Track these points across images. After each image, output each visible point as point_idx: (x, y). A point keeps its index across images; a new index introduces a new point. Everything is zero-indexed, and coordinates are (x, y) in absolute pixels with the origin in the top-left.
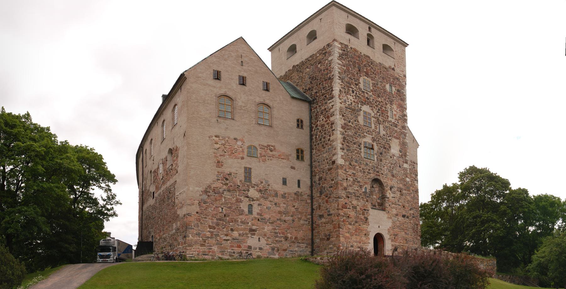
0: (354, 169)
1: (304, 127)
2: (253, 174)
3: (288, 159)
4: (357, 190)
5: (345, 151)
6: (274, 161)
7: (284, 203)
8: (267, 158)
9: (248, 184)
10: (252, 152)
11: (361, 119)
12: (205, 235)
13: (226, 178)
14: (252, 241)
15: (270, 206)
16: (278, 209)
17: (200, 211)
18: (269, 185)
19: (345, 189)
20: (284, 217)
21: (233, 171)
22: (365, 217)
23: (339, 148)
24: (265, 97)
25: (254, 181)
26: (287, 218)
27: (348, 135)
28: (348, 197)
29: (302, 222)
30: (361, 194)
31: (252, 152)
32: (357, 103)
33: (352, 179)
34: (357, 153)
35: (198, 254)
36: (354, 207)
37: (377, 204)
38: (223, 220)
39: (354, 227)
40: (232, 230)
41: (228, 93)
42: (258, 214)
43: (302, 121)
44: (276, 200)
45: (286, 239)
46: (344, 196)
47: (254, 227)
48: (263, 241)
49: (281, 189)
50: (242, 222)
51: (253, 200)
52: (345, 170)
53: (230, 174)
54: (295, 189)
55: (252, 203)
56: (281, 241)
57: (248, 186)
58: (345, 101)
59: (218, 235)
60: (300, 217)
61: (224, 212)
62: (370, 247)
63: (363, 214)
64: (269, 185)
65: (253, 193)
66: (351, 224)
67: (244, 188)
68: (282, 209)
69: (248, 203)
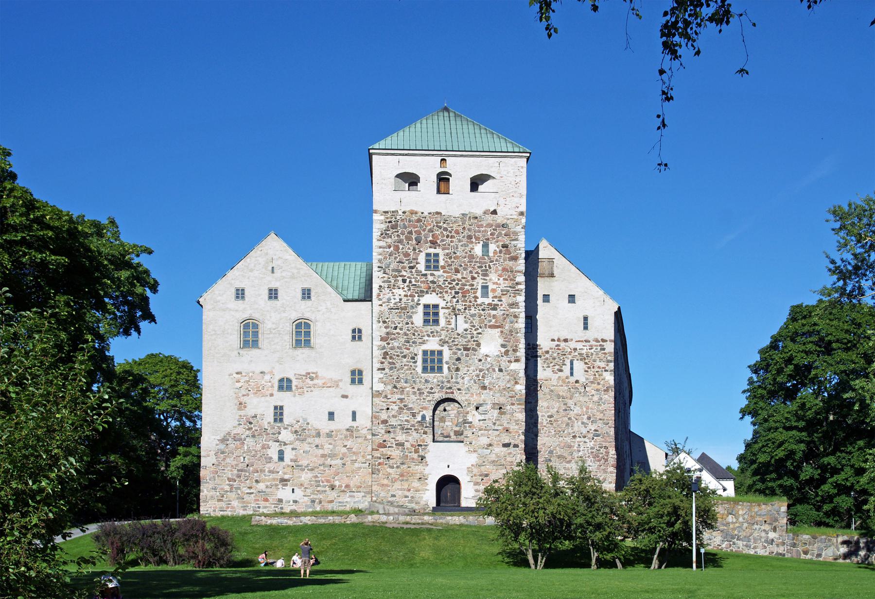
0: (402, 392)
1: (363, 338)
3: (337, 386)
4: (407, 421)
5: (387, 370)
6: (316, 392)
8: (305, 389)
9: (279, 425)
10: (285, 385)
14: (285, 493)
15: (309, 449)
16: (321, 452)
17: (216, 463)
18: (308, 424)
19: (385, 422)
20: (329, 461)
21: (259, 412)
22: (419, 456)
24: (304, 309)
25: (286, 420)
26: (333, 463)
29: (356, 465)
30: (413, 426)
31: (285, 385)
33: (396, 408)
35: (214, 511)
36: (402, 445)
37: (452, 434)
38: (245, 471)
40: (257, 481)
42: (292, 460)
43: (360, 331)
44: (317, 441)
46: (383, 431)
47: (286, 477)
48: (299, 494)
49: (325, 426)
50: (270, 472)
51: (285, 444)
52: (386, 396)
53: (255, 416)
54: (349, 422)
55: (283, 448)
57: (279, 428)
58: (389, 299)
59: (239, 488)
62: (430, 497)
64: (308, 424)
65: (286, 435)
66: (392, 467)
67: (273, 431)
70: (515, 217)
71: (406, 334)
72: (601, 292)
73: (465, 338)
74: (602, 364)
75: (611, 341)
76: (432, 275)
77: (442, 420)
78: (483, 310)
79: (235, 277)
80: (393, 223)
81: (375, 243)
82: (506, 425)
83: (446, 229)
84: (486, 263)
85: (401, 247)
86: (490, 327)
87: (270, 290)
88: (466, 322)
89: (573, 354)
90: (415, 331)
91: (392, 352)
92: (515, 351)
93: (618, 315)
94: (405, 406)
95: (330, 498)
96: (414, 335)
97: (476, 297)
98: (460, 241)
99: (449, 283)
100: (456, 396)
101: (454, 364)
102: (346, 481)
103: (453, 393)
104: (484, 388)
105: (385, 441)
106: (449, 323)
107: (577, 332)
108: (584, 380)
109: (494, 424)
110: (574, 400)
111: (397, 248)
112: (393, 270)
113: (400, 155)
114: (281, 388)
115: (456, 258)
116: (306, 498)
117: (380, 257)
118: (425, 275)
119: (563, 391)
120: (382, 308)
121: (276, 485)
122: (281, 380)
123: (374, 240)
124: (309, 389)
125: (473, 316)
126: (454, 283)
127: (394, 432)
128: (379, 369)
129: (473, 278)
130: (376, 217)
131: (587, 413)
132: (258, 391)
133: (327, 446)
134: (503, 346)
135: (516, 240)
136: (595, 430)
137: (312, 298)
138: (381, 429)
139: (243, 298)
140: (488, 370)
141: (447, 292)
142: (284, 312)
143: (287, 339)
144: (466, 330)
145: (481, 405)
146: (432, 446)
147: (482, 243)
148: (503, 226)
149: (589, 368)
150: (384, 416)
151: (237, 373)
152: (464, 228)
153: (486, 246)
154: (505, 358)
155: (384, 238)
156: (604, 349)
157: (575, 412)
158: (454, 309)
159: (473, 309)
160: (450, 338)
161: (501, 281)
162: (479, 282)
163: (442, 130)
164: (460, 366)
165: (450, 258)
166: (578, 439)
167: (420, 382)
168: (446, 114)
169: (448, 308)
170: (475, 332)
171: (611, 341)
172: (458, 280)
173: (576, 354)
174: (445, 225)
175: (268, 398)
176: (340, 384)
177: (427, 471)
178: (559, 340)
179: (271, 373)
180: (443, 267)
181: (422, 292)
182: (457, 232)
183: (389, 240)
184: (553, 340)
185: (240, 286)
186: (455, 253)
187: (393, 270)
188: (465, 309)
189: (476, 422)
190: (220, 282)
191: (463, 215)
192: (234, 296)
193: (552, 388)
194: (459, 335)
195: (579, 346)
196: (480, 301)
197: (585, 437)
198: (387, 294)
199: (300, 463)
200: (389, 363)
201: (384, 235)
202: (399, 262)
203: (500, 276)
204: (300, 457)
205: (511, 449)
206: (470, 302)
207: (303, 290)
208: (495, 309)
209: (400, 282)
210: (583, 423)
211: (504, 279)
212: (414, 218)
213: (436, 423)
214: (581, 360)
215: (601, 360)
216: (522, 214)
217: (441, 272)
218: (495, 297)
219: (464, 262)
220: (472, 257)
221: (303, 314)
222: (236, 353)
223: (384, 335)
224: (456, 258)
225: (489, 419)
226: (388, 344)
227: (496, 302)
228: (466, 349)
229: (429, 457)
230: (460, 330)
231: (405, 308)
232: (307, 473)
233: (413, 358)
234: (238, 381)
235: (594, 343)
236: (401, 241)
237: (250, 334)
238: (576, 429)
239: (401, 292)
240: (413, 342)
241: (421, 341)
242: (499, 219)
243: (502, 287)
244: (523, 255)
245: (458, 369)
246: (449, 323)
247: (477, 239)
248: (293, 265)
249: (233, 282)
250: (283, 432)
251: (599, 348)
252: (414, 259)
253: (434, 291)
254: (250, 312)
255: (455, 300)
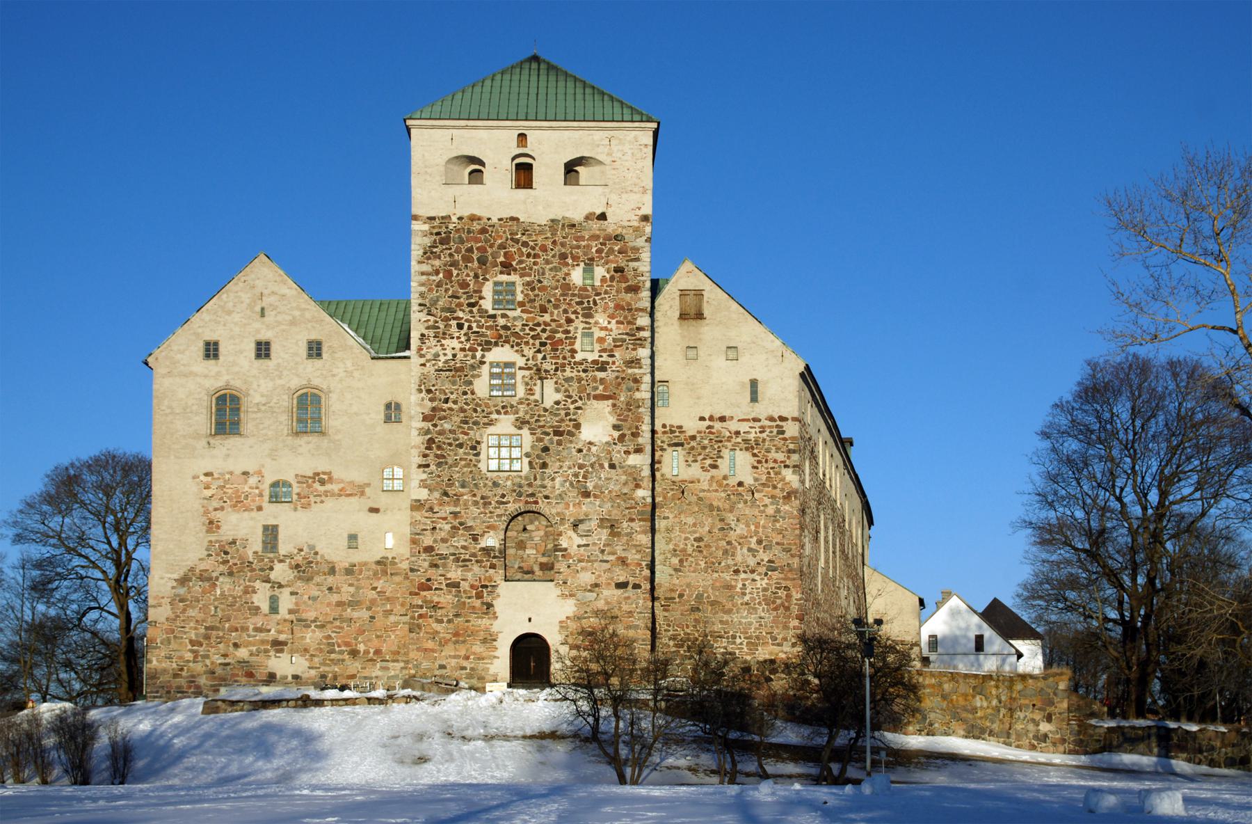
0: (456, 503)
2: (281, 537)
3: (362, 493)
4: (464, 547)
5: (433, 467)
6: (330, 503)
7: (350, 585)
8: (312, 499)
9: (272, 555)
10: (278, 492)
11: (482, 386)
12: (181, 658)
13: (224, 550)
15: (317, 593)
16: (335, 598)
18: (316, 553)
19: (429, 549)
21: (240, 534)
23: (415, 466)
24: (311, 373)
25: (283, 549)
26: (355, 615)
27: (441, 433)
28: (436, 566)
29: (392, 618)
30: (474, 555)
31: (278, 492)
32: (470, 350)
33: (447, 527)
34: (468, 465)
36: (456, 585)
37: (536, 568)
38: (217, 629)
39: (451, 626)
40: (236, 645)
41: (232, 383)
42: (290, 612)
43: (398, 406)
44: (330, 580)
45: (354, 653)
46: (426, 564)
47: (282, 637)
50: (257, 630)
51: (280, 586)
52: (431, 509)
53: (234, 542)
56: (343, 660)
58: (437, 355)
59: (207, 657)
60: (388, 607)
61: (220, 614)
63: (479, 596)
65: (281, 572)
66: (441, 621)
68: (345, 597)
69: (269, 594)
70: (636, 224)
71: (462, 410)
72: (778, 343)
73: (556, 415)
74: (780, 456)
75: (794, 419)
76: (504, 316)
77: (521, 545)
78: (585, 371)
79: (204, 324)
80: (443, 233)
81: (415, 267)
82: (620, 553)
83: (525, 244)
84: (589, 297)
85: (455, 272)
86: (597, 397)
87: (259, 344)
88: (557, 390)
89: (733, 440)
90: (477, 405)
91: (441, 438)
92: (635, 435)
93: (807, 377)
94: (461, 524)
95: (351, 671)
96: (475, 411)
97: (573, 351)
98: (547, 262)
99: (531, 329)
100: (543, 506)
101: (538, 457)
102: (376, 643)
103: (536, 502)
104: (586, 494)
105: (429, 580)
106: (530, 391)
107: (740, 407)
108: (752, 482)
109: (603, 552)
110: (736, 513)
111: (448, 275)
112: (443, 310)
113: (454, 127)
114: (275, 498)
115: (543, 289)
116: (313, 672)
117: (423, 289)
118: (494, 316)
119: (718, 498)
120: (425, 370)
121: (266, 651)
122: (275, 485)
123: (413, 263)
124: (318, 499)
125: (567, 380)
126: (539, 329)
127: (445, 566)
128: (420, 466)
129: (569, 321)
130: (417, 226)
131: (756, 533)
132: (239, 503)
133: (345, 588)
134: (616, 427)
135: (637, 260)
136: (770, 561)
137: (325, 355)
138: (424, 562)
139: (216, 356)
140: (592, 465)
141: (527, 343)
142: (280, 378)
143: (284, 421)
144: (557, 403)
145: (581, 521)
146: (504, 588)
147: (582, 264)
148: (616, 237)
149: (759, 462)
150: (428, 540)
151: (206, 475)
152: (554, 243)
153: (589, 270)
154: (619, 447)
155: (429, 258)
156: (783, 432)
157: (738, 531)
158: (539, 370)
159: (568, 369)
160: (532, 416)
161: (613, 325)
162: (579, 324)
163: (524, 90)
164: (548, 461)
165: (533, 289)
166: (743, 576)
167: (485, 485)
168: (534, 65)
169: (529, 369)
170: (572, 407)
171: (794, 419)
172: (546, 324)
173: (739, 440)
174: (524, 238)
175: (254, 514)
176: (367, 490)
177: (496, 626)
178: (711, 418)
179: (259, 473)
180: (521, 304)
181: (488, 343)
182: (544, 248)
183: (437, 263)
184: (702, 419)
185: (211, 337)
186: (540, 281)
187: (443, 310)
188: (556, 370)
189: (573, 550)
190: (180, 331)
191: (552, 221)
192: (201, 353)
193: (701, 495)
194: (546, 410)
195: (744, 427)
196: (579, 357)
197: (753, 572)
198: (432, 347)
199: (304, 616)
200: (437, 456)
201: (429, 254)
202: (454, 296)
203: (612, 316)
204: (302, 607)
205: (630, 591)
206: (564, 358)
207: (310, 343)
208: (603, 367)
209: (454, 329)
210: (750, 550)
211: (618, 322)
212: (476, 226)
213: (511, 552)
214: (747, 449)
215: (778, 450)
216: (645, 218)
217: (518, 313)
218: (604, 350)
219: (554, 295)
220: (566, 287)
221: (309, 380)
222: (203, 442)
223: (427, 411)
224: (543, 289)
225: (594, 544)
226: (435, 425)
227: (605, 358)
228: (557, 433)
229: (499, 605)
230: (548, 403)
231: (461, 369)
232: (314, 631)
233: (474, 448)
234: (207, 487)
235: (768, 423)
236: (454, 264)
237: (227, 413)
238: (739, 558)
239: (455, 343)
240: (476, 423)
241: (486, 420)
242: (611, 226)
243: (615, 333)
244: (648, 284)
245: (544, 465)
246: (530, 391)
247: (575, 258)
248: (294, 305)
249: (200, 330)
250: (278, 567)
251: (775, 430)
252: (475, 292)
253: (508, 342)
254: (226, 378)
255: (540, 356)
